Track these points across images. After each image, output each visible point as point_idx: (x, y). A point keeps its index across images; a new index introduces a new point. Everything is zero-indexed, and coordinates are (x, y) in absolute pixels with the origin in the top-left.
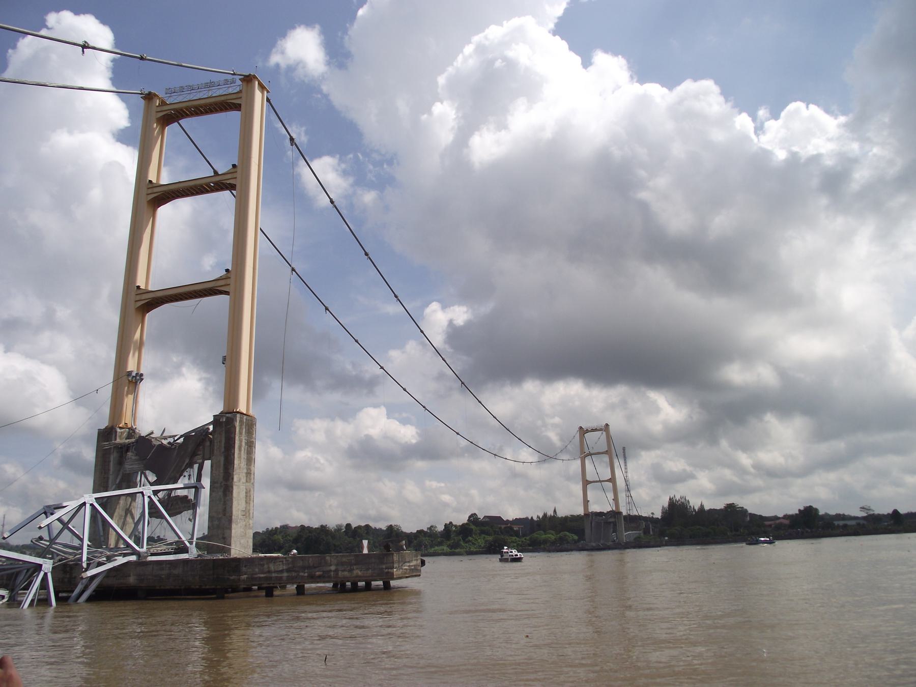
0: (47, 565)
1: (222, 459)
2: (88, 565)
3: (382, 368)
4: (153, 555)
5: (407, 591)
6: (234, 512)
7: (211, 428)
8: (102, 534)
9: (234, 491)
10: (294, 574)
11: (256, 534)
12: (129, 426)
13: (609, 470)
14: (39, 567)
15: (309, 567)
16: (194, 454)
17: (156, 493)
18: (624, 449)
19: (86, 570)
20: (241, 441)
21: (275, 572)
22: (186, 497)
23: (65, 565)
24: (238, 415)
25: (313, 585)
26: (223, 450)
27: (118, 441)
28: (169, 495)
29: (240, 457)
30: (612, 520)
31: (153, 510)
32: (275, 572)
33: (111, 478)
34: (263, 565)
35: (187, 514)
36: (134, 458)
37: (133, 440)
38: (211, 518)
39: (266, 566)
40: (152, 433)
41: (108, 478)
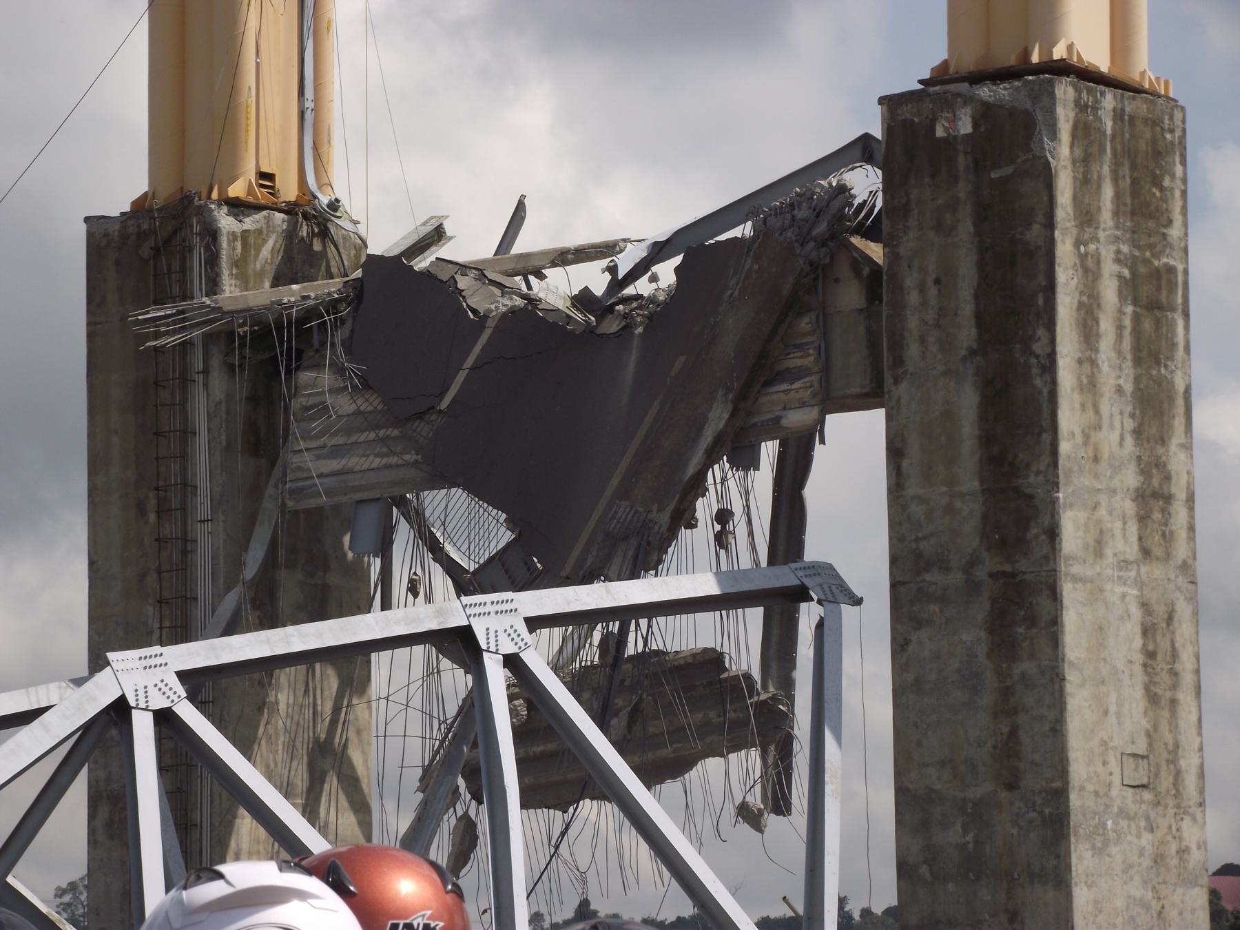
1: (968, 401)
6: (1080, 768)
7: (864, 183)
9: (1070, 619)
12: (289, 191)
16: (760, 371)
20: (1089, 271)
22: (712, 660)
24: (1065, 90)
26: (967, 334)
27: (231, 292)
28: (613, 646)
29: (1090, 386)
33: (208, 541)
35: (731, 774)
36: (345, 405)
37: (330, 287)
38: (912, 803)
40: (437, 235)
41: (186, 544)
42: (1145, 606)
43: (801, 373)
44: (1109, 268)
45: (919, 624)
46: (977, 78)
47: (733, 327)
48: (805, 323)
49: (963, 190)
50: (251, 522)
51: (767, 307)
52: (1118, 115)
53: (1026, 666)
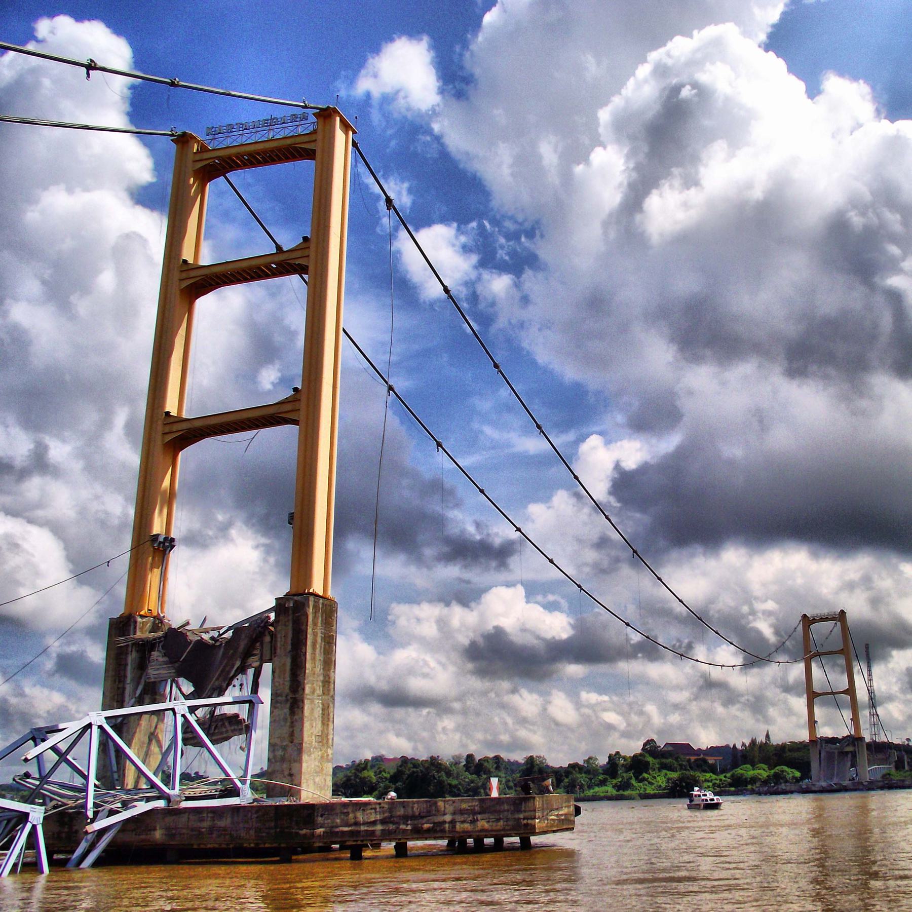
0: (37, 814)
1: (288, 661)
2: (96, 814)
3: (518, 530)
4: (188, 799)
5: (554, 851)
6: (306, 738)
7: (272, 616)
8: (115, 769)
9: (306, 708)
10: (392, 827)
11: (336, 770)
12: (155, 614)
13: (845, 678)
14: (26, 815)
15: (413, 817)
16: (248, 654)
17: (192, 709)
18: (867, 647)
19: (93, 821)
21: (364, 824)
22: (236, 716)
23: (62, 814)
24: (312, 598)
25: (420, 843)
26: (289, 647)
27: (139, 635)
28: (212, 713)
29: (314, 659)
30: (850, 749)
31: (189, 735)
32: (364, 824)
33: (129, 689)
34: (348, 814)
35: (238, 740)
36: (161, 659)
37: (160, 634)
38: (272, 746)
39: (351, 815)
40: (188, 623)
41: (124, 689)
42: (323, 704)
43: (255, 655)
44: (319, 635)
45: (275, 708)
46: (294, 595)
47: (243, 644)
48: (258, 644)
49: (290, 617)
50: (138, 684)
51: (252, 641)
52: (323, 604)
53: (296, 717)
